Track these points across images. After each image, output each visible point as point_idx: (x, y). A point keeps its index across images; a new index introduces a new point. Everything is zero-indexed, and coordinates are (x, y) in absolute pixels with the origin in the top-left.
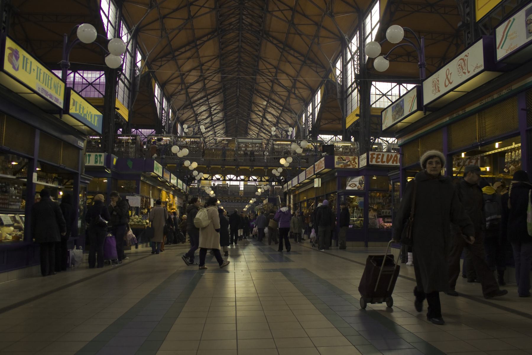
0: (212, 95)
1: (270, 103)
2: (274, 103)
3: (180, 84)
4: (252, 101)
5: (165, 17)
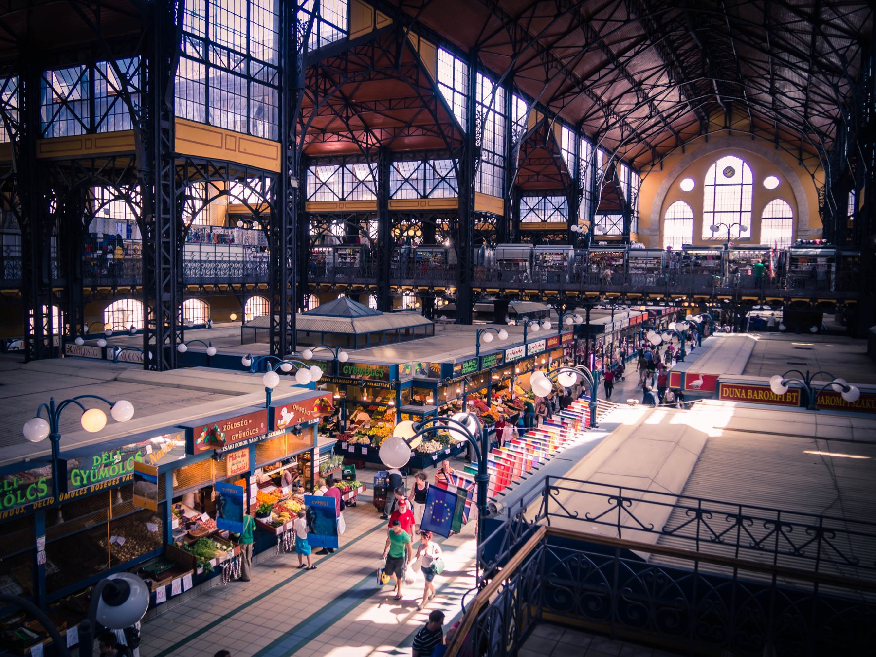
5: (550, 46)
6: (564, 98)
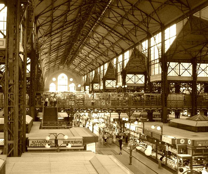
2: (96, 51)
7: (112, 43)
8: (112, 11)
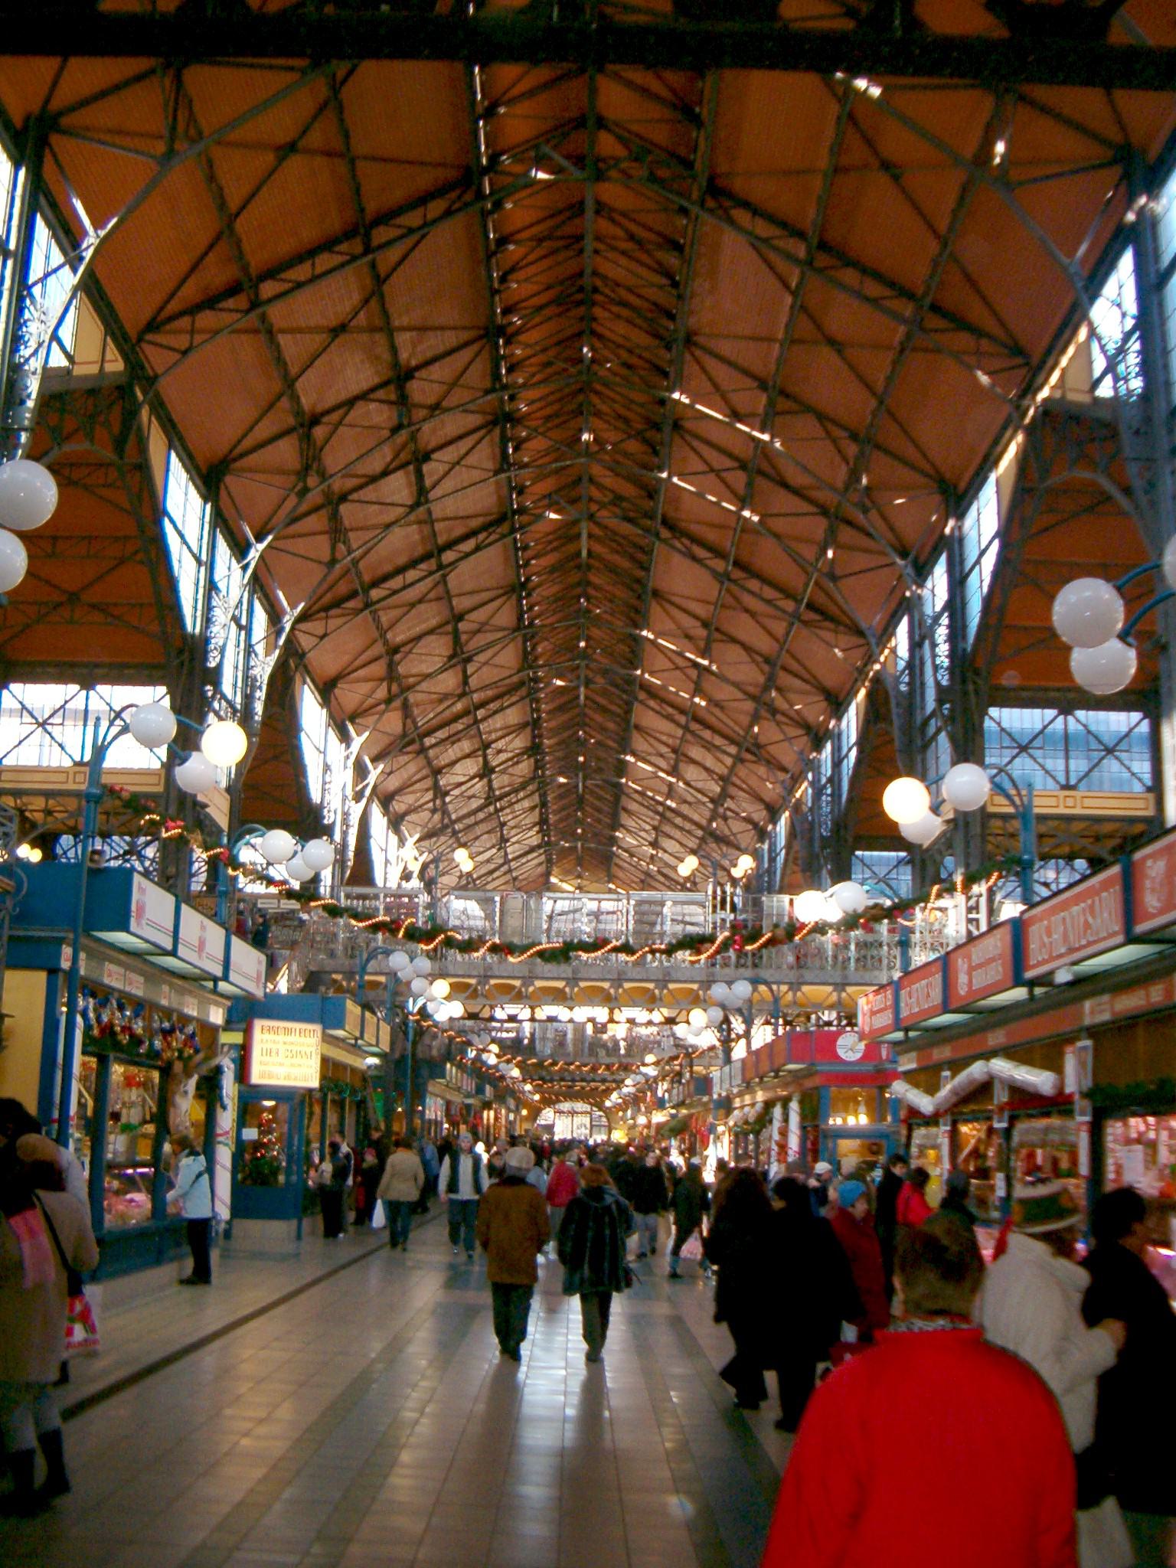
0: (493, 706)
1: (692, 733)
2: (707, 734)
3: (382, 680)
4: (633, 721)
5: (343, 498)
6: (327, 617)
7: (767, 660)
8: (695, 443)
